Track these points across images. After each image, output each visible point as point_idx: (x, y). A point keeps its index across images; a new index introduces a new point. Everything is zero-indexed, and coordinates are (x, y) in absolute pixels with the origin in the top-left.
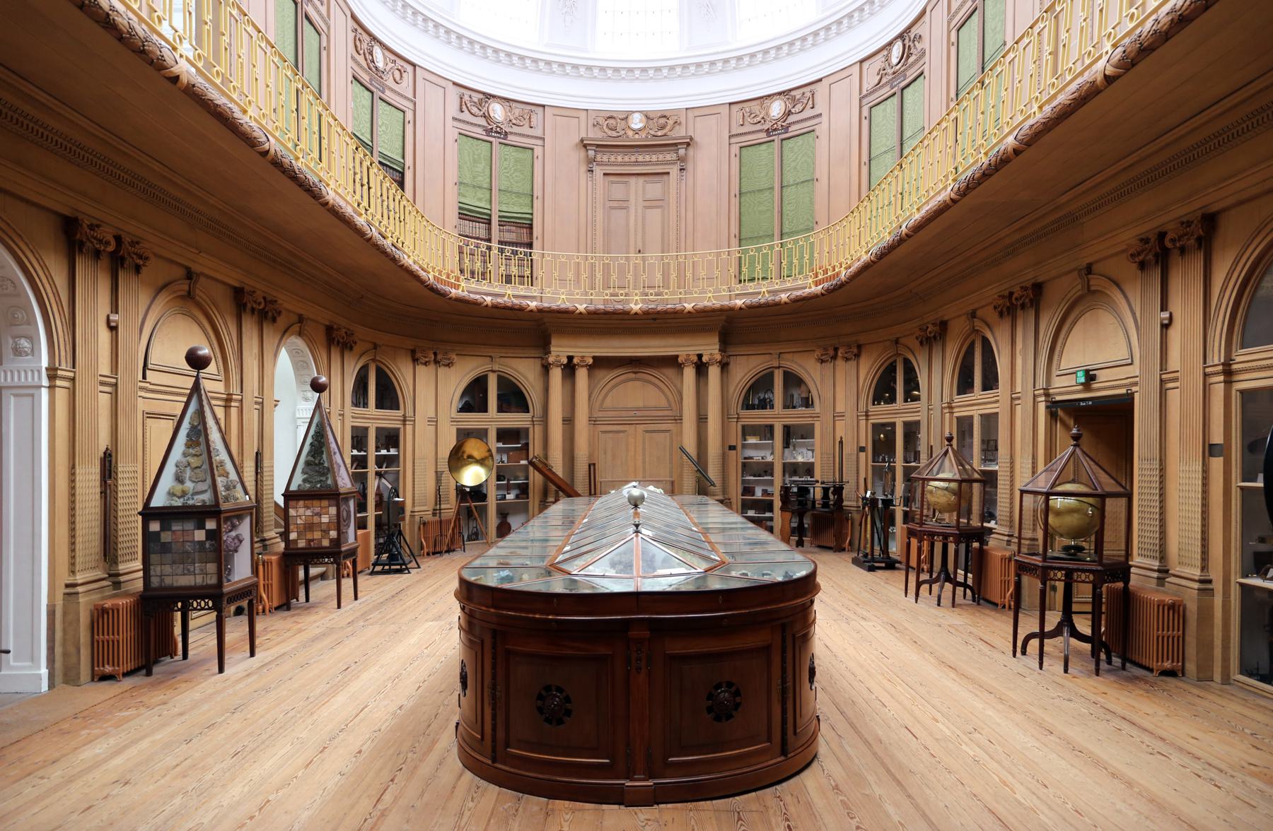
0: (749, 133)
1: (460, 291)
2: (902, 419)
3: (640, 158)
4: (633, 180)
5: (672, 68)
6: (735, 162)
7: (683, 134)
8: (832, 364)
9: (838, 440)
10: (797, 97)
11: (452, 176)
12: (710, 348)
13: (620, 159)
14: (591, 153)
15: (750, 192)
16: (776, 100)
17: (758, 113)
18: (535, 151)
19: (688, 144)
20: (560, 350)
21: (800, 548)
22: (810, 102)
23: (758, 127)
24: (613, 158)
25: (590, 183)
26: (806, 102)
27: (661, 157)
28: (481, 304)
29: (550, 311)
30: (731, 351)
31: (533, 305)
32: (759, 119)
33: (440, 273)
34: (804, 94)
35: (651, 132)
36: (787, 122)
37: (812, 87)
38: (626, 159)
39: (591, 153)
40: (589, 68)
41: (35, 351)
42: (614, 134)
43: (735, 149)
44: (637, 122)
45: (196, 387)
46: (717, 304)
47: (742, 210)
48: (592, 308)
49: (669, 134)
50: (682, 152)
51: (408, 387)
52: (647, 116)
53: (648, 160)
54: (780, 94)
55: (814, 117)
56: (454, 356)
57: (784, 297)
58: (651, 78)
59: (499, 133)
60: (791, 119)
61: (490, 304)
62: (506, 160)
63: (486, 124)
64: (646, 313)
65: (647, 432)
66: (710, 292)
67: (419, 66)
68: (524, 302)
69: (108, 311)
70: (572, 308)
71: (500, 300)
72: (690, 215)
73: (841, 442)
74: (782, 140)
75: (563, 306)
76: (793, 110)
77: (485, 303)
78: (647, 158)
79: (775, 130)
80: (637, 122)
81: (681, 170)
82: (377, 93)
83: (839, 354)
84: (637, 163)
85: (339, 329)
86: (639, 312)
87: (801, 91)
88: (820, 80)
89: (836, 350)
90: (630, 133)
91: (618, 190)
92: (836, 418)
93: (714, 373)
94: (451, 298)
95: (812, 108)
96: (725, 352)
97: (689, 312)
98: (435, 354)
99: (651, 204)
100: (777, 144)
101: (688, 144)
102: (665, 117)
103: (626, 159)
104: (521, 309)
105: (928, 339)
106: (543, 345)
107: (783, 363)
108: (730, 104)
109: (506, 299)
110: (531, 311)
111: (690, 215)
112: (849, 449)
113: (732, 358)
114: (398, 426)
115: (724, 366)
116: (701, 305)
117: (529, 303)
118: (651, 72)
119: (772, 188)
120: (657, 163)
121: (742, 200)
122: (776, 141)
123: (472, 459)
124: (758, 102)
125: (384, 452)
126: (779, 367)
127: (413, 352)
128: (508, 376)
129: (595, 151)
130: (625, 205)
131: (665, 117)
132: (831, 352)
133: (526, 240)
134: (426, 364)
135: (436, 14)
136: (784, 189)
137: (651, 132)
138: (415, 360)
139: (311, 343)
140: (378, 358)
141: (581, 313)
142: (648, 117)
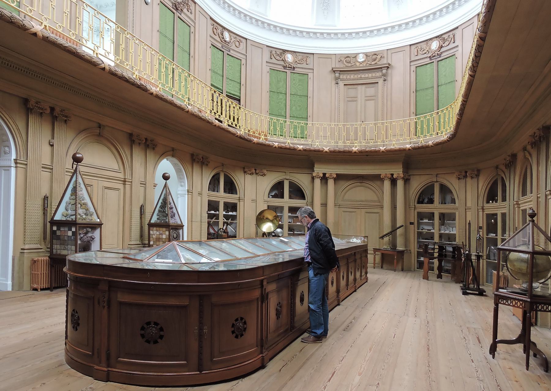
0: (420, 59)
1: (261, 140)
2: (501, 211)
3: (363, 76)
4: (359, 87)
5: (379, 30)
6: (413, 75)
7: (386, 62)
9: (468, 222)
10: (446, 38)
11: (266, 87)
12: (398, 171)
13: (352, 77)
14: (337, 75)
15: (421, 90)
16: (435, 40)
17: (425, 48)
18: (309, 75)
19: (388, 67)
20: (319, 170)
21: (439, 279)
22: (453, 40)
23: (425, 56)
24: (348, 77)
25: (337, 89)
26: (450, 40)
27: (374, 75)
28: (272, 146)
29: (310, 151)
31: (301, 147)
32: (425, 51)
33: (249, 131)
34: (449, 36)
35: (368, 62)
36: (440, 52)
37: (453, 32)
38: (356, 77)
39: (337, 75)
40: (336, 34)
41: (10, 152)
42: (350, 65)
43: (413, 68)
44: (361, 58)
46: (397, 147)
47: (417, 99)
48: (332, 149)
49: (378, 63)
50: (384, 71)
51: (241, 185)
52: (367, 55)
53: (367, 77)
54: (436, 37)
55: (454, 48)
56: (265, 172)
57: (430, 143)
58: (368, 36)
59: (290, 68)
60: (443, 50)
61: (277, 146)
62: (294, 80)
63: (284, 64)
64: (361, 152)
65: (367, 213)
66: (394, 141)
67: (248, 39)
68: (296, 146)
69: (50, 138)
70: (321, 149)
71: (283, 145)
72: (389, 103)
73: (470, 224)
74: (438, 61)
75: (317, 148)
76: (443, 45)
77: (274, 146)
78: (367, 75)
79: (434, 56)
80: (361, 58)
81: (384, 80)
82: (226, 52)
83: (468, 175)
84: (361, 78)
85: (197, 155)
86: (357, 151)
87: (447, 35)
88: (457, 28)
89: (466, 172)
90: (358, 64)
91: (352, 92)
92: (467, 210)
94: (254, 143)
95: (454, 43)
97: (383, 152)
98: (256, 170)
99: (369, 98)
100: (435, 64)
101: (388, 67)
102: (376, 54)
103: (356, 77)
104: (294, 149)
106: (311, 168)
108: (410, 45)
109: (287, 144)
110: (300, 150)
111: (389, 103)
112: (474, 227)
116: (389, 148)
117: (298, 146)
118: (368, 33)
119: (433, 87)
120: (372, 78)
121: (417, 94)
122: (435, 62)
123: (268, 220)
124: (425, 42)
125: (213, 212)
127: (244, 168)
128: (294, 182)
129: (339, 74)
130: (355, 99)
131: (376, 54)
132: (464, 174)
133: (304, 116)
134: (250, 174)
135: (256, 15)
136: (439, 87)
137: (368, 62)
138: (245, 172)
139: (181, 160)
140: (224, 170)
141: (326, 152)
142: (367, 56)
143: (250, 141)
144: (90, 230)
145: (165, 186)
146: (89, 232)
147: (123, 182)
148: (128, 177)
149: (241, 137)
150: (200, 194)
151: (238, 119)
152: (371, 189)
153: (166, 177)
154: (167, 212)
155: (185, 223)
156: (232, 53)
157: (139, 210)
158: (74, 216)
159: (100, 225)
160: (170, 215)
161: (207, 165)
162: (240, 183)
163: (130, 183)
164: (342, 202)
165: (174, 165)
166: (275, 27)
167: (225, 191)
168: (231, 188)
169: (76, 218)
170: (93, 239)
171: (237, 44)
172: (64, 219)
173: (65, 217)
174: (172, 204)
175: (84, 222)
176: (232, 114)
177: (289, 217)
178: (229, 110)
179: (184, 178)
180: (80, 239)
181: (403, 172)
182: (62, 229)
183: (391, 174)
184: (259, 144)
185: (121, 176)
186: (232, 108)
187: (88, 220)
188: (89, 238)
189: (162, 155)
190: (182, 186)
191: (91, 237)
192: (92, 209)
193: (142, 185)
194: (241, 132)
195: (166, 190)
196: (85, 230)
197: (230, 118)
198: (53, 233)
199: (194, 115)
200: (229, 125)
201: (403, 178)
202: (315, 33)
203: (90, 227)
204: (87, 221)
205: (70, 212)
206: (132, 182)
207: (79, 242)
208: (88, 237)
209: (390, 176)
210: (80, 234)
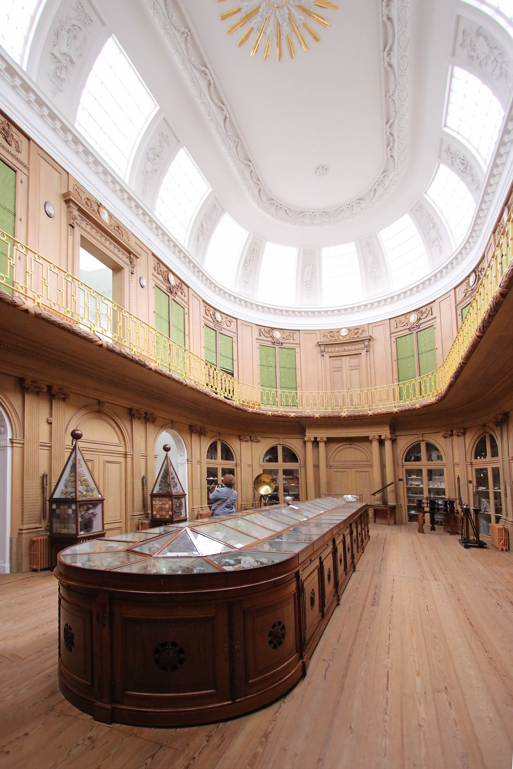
8: (451, 438)
12: (385, 432)
30: (397, 433)
45: (75, 447)
93: (388, 444)
96: (394, 434)
105: (499, 422)
107: (425, 439)
113: (398, 437)
114: (233, 468)
115: (394, 441)
125: (212, 478)
126: (423, 441)
143: (245, 411)
144: (91, 506)
145: (166, 456)
146: (90, 508)
147: (124, 456)
148: (129, 450)
149: (236, 408)
150: (200, 462)
151: (233, 391)
152: (360, 450)
153: (166, 449)
154: (169, 483)
155: (187, 492)
156: (224, 331)
157: (141, 481)
158: (74, 494)
159: (102, 501)
160: (172, 485)
161: (205, 435)
162: (236, 449)
163: (131, 456)
164: (334, 463)
165: (174, 437)
166: (263, 307)
167: (222, 458)
168: (228, 454)
169: (76, 495)
170: (95, 515)
171: (228, 323)
172: (63, 497)
173: (65, 494)
174: (174, 474)
175: (84, 499)
176: (227, 386)
177: (284, 479)
178: (225, 384)
179: (183, 448)
180: (81, 517)
181: (390, 433)
182: (62, 507)
183: (379, 436)
184: (253, 413)
185: (122, 449)
186: (227, 381)
187: (89, 497)
188: (90, 515)
189: (162, 427)
190: (181, 455)
191: (92, 513)
192: (93, 486)
193: (143, 457)
194: (236, 402)
195: (168, 461)
196: (86, 507)
197: (226, 391)
198: (52, 511)
199: (192, 388)
200: (225, 397)
201: (391, 439)
202: (300, 312)
203: (91, 504)
204: (89, 497)
205: (70, 489)
206: (133, 455)
207: (80, 520)
208: (89, 514)
209: (378, 437)
210: (81, 511)
